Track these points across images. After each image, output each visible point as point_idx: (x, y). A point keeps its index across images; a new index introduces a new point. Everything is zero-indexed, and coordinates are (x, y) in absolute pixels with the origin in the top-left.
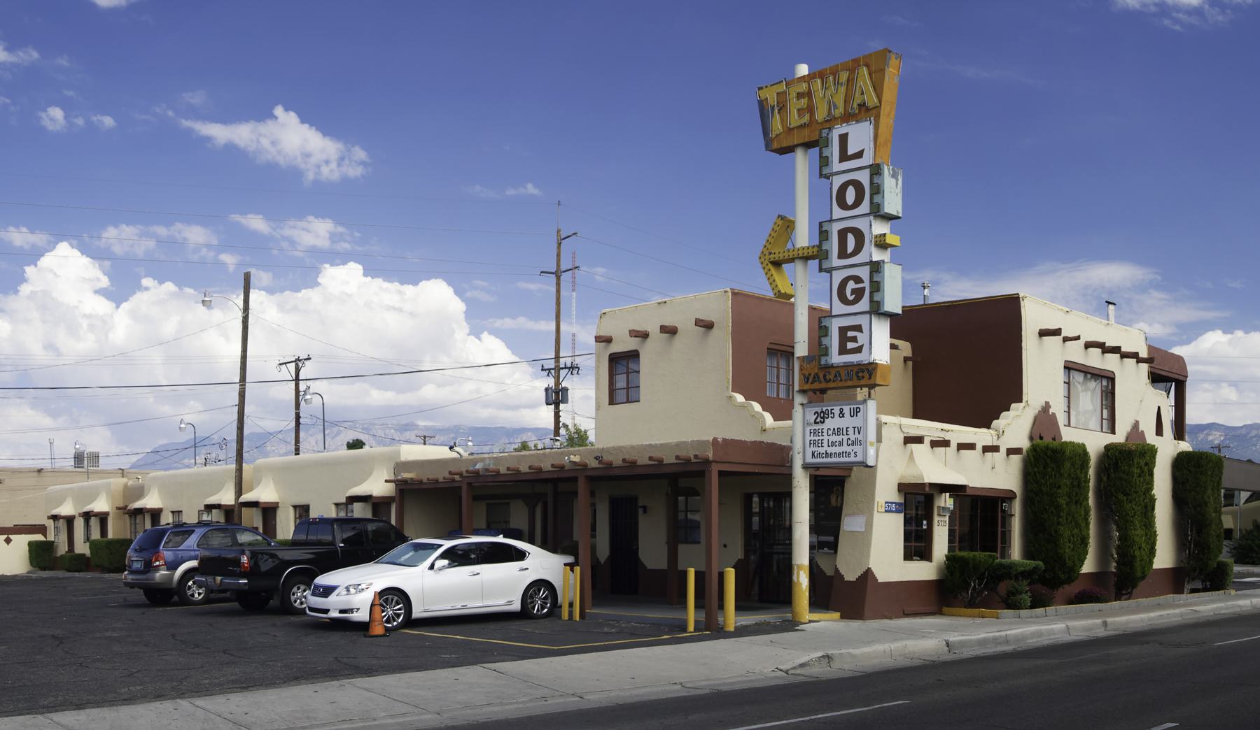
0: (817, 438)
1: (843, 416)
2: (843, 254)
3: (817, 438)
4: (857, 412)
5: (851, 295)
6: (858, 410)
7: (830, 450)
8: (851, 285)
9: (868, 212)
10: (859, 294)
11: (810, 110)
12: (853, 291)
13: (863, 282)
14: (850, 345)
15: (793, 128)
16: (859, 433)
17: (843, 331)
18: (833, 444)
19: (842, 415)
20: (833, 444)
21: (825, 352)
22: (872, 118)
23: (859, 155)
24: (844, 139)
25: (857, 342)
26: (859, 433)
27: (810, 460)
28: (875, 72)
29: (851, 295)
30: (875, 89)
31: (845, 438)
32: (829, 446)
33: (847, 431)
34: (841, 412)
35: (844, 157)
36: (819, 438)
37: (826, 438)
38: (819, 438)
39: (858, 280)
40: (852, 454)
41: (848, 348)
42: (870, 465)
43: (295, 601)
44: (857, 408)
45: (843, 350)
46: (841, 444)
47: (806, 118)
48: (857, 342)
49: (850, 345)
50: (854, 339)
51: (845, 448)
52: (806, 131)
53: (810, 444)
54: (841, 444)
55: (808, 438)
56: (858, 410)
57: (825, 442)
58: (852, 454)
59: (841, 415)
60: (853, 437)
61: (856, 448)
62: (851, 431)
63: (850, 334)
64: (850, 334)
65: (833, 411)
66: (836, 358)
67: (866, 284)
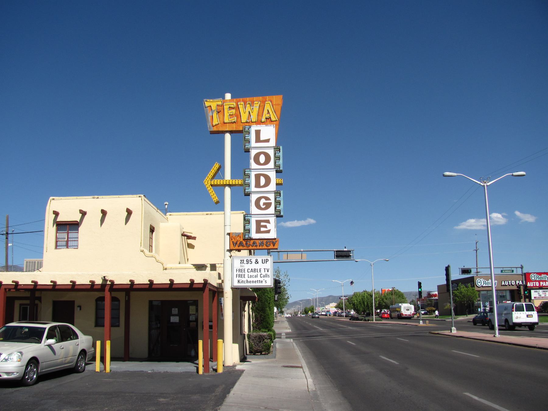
0: (241, 273)
1: (258, 263)
2: (258, 185)
3: (241, 273)
4: (266, 261)
5: (263, 205)
6: (267, 260)
7: (249, 279)
8: (263, 201)
9: (273, 168)
10: (268, 206)
11: (239, 116)
12: (264, 204)
13: (270, 200)
14: (263, 229)
15: (226, 123)
16: (268, 272)
17: (258, 223)
18: (251, 276)
19: (257, 262)
20: (251, 276)
21: (249, 231)
22: (274, 125)
23: (268, 141)
24: (258, 133)
25: (267, 228)
26: (268, 272)
27: (236, 284)
28: (275, 105)
29: (263, 205)
30: (275, 113)
31: (259, 274)
32: (248, 277)
33: (260, 270)
34: (256, 261)
35: (258, 140)
36: (242, 273)
37: (246, 273)
38: (242, 273)
39: (267, 198)
40: (264, 282)
41: (261, 224)
42: (253, 238)
43: (28, 379)
44: (266, 259)
45: (258, 231)
46: (256, 276)
47: (234, 119)
48: (267, 228)
49: (263, 229)
50: (265, 227)
51: (259, 278)
52: (234, 125)
53: (237, 276)
54: (256, 276)
55: (235, 273)
56: (267, 260)
57: (246, 276)
58: (264, 282)
59: (256, 263)
60: (264, 273)
61: (266, 279)
62: (263, 271)
63: (262, 224)
64: (262, 224)
65: (251, 260)
66: (254, 235)
67: (273, 201)
